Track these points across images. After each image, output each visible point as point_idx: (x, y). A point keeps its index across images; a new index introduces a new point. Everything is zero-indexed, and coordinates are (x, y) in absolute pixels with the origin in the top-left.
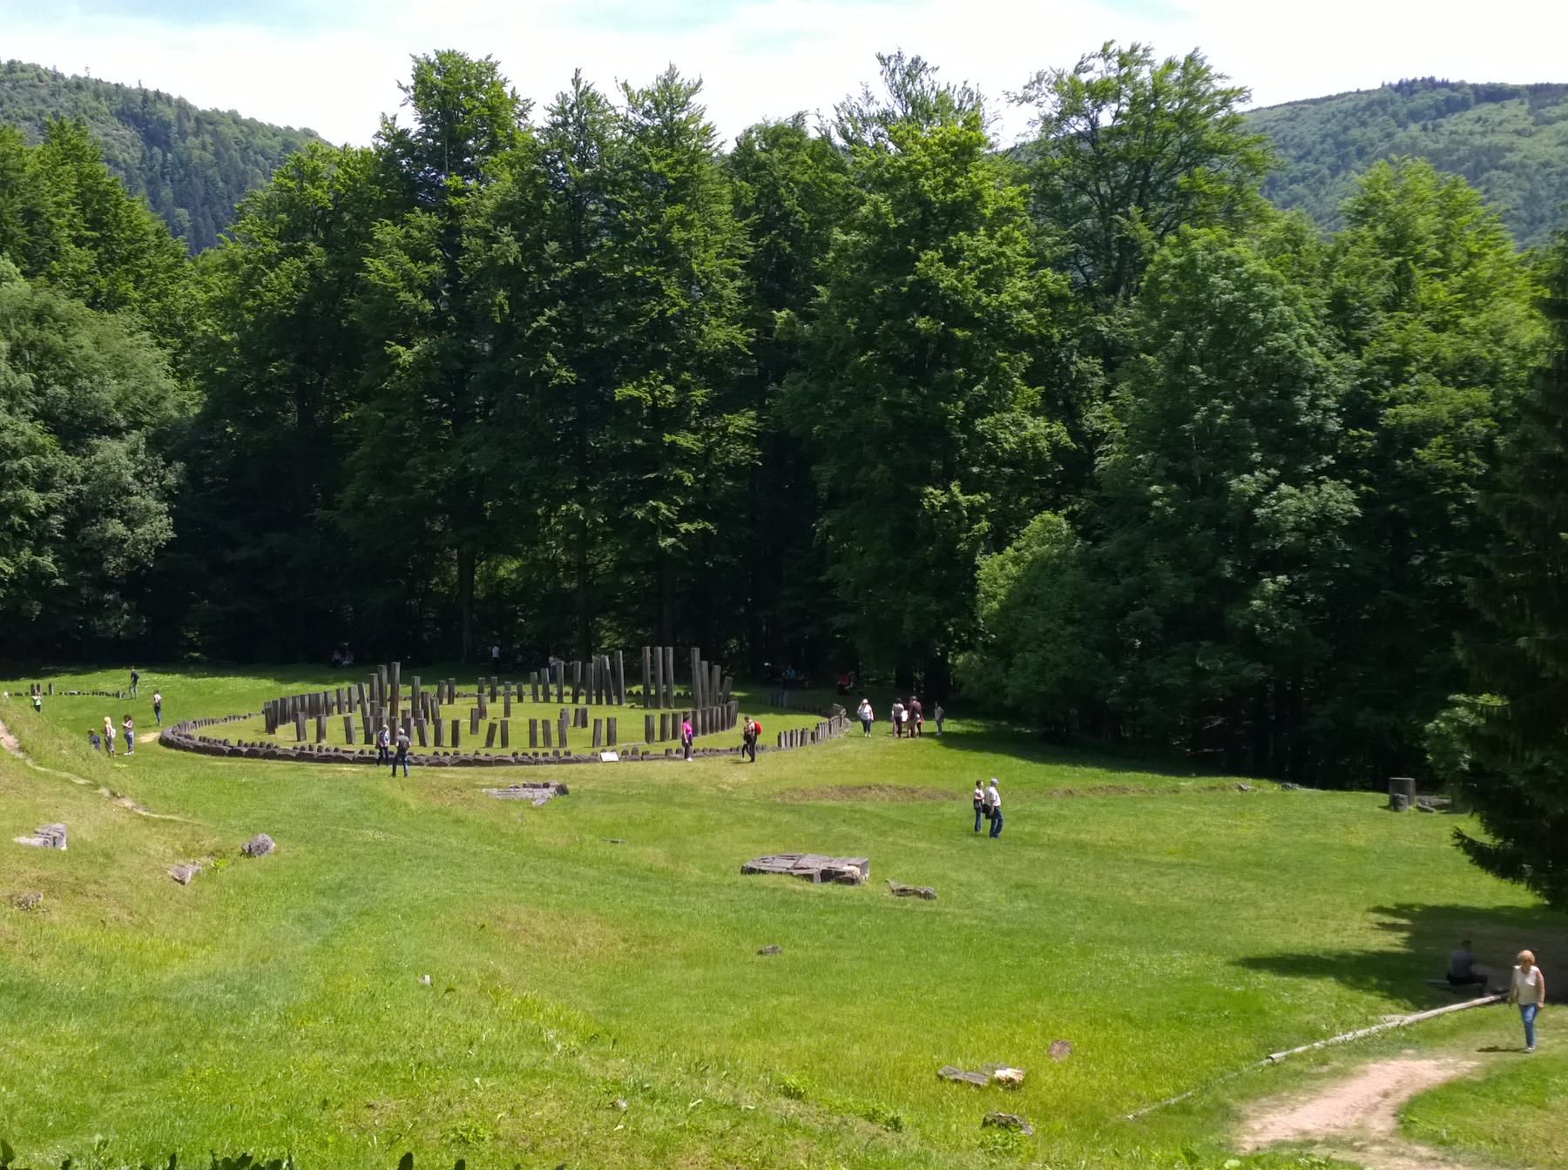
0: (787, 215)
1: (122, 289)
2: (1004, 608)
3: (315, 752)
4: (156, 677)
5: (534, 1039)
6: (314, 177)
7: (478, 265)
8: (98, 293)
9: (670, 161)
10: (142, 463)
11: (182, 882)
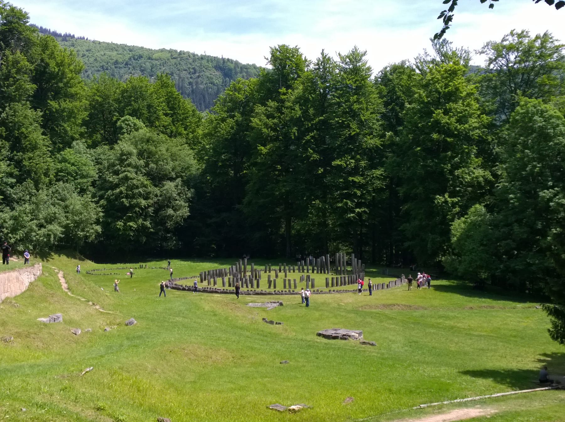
0: (398, 98)
2: (459, 240)
4: (182, 262)
6: (239, 90)
7: (287, 118)
8: (172, 132)
9: (354, 80)
10: (180, 189)
11: (76, 334)
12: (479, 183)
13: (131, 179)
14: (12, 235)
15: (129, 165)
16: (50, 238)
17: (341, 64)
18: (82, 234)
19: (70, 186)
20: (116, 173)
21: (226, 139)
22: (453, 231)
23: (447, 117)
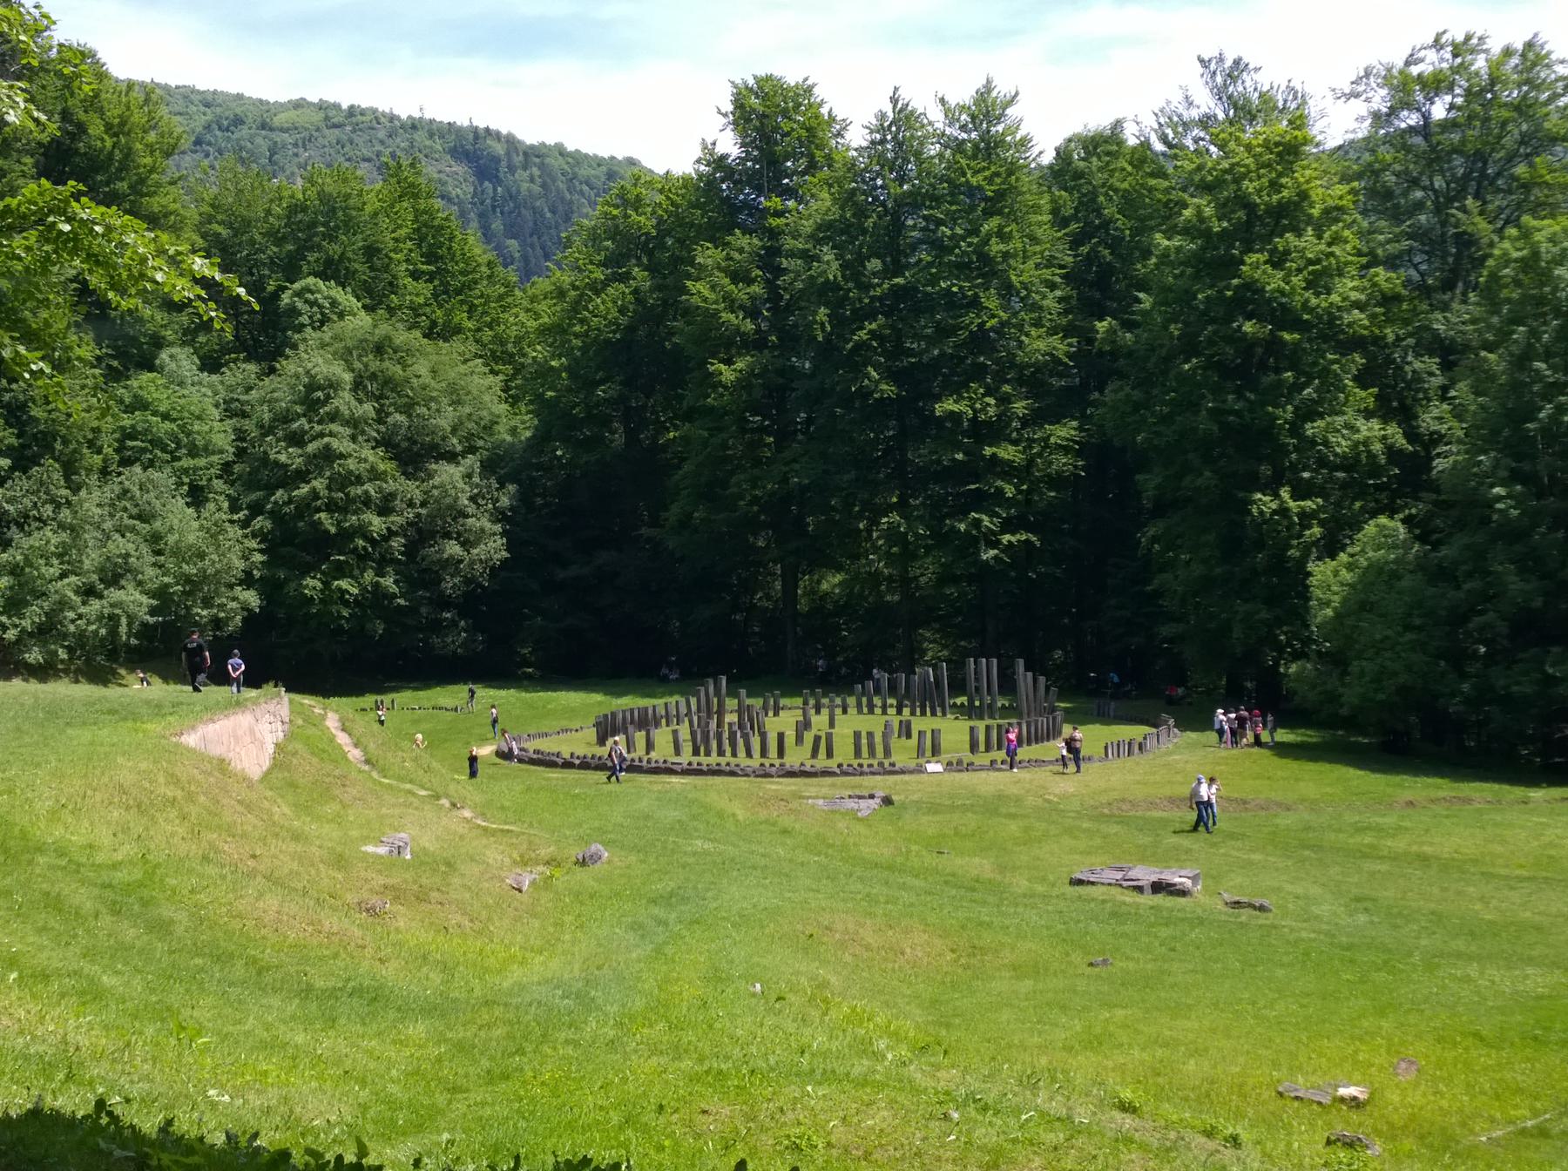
0: (1106, 224)
1: (456, 320)
2: (1339, 616)
3: (644, 763)
4: (492, 692)
8: (434, 323)
9: (987, 173)
10: (477, 486)
13: (342, 456)
14: (9, 618)
15: (334, 417)
16: (118, 625)
18: (205, 613)
19: (163, 477)
20: (297, 439)
21: (608, 342)
22: (1318, 593)
23: (1281, 274)
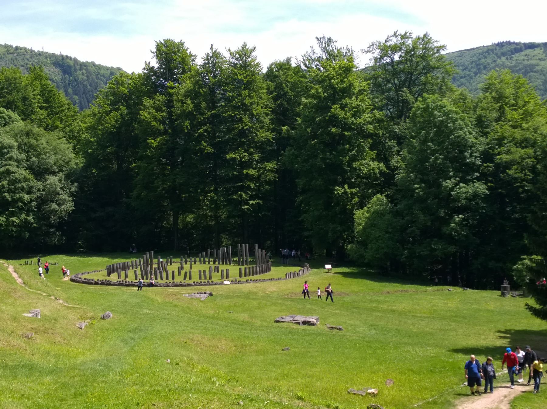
0: (285, 93)
1: (56, 124)
2: (364, 229)
3: (124, 283)
4: (68, 258)
5: (208, 380)
6: (122, 84)
8: (48, 125)
9: (245, 75)
10: (63, 184)
11: (81, 329)
12: (374, 173)
13: (13, 173)
15: (11, 159)
17: (231, 60)
21: (111, 132)
22: (357, 221)
